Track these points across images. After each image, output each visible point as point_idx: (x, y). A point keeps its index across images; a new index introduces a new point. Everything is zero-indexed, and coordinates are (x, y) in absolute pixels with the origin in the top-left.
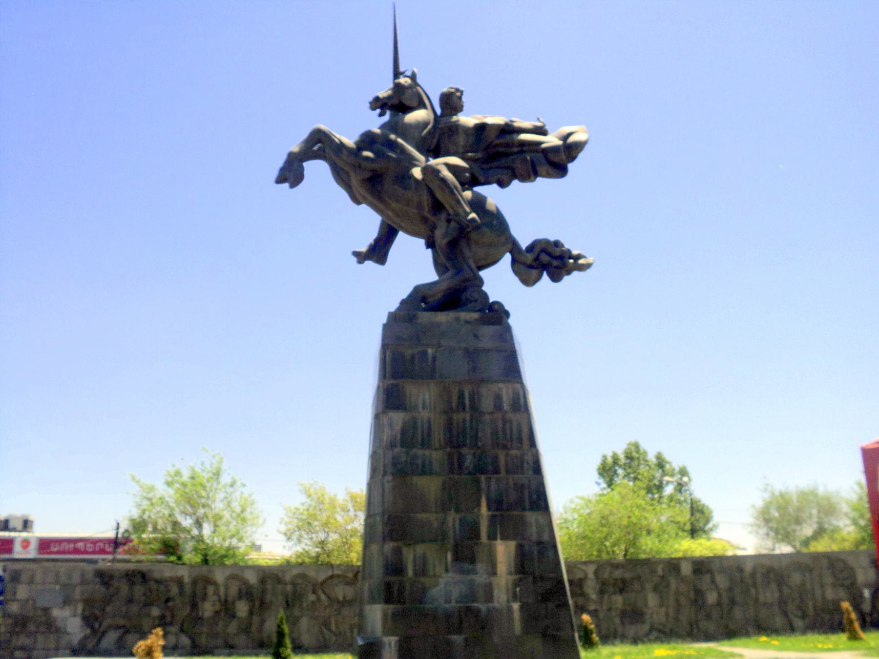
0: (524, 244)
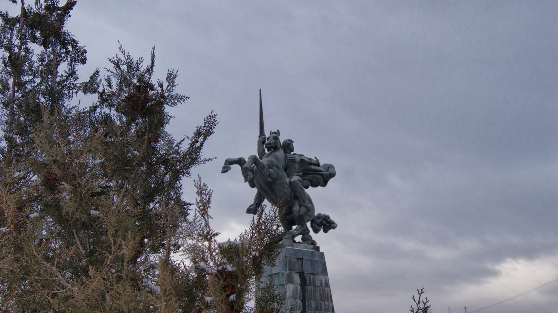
0: (316, 214)
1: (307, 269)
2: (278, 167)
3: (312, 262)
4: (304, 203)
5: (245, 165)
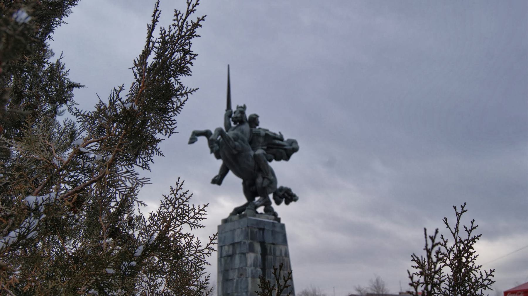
0: (278, 186)
1: (269, 239)
2: (243, 140)
3: (274, 233)
4: (267, 174)
5: (211, 137)
